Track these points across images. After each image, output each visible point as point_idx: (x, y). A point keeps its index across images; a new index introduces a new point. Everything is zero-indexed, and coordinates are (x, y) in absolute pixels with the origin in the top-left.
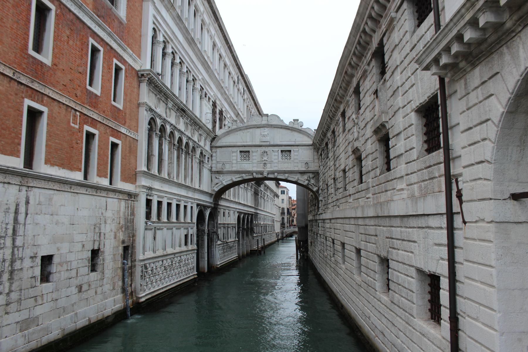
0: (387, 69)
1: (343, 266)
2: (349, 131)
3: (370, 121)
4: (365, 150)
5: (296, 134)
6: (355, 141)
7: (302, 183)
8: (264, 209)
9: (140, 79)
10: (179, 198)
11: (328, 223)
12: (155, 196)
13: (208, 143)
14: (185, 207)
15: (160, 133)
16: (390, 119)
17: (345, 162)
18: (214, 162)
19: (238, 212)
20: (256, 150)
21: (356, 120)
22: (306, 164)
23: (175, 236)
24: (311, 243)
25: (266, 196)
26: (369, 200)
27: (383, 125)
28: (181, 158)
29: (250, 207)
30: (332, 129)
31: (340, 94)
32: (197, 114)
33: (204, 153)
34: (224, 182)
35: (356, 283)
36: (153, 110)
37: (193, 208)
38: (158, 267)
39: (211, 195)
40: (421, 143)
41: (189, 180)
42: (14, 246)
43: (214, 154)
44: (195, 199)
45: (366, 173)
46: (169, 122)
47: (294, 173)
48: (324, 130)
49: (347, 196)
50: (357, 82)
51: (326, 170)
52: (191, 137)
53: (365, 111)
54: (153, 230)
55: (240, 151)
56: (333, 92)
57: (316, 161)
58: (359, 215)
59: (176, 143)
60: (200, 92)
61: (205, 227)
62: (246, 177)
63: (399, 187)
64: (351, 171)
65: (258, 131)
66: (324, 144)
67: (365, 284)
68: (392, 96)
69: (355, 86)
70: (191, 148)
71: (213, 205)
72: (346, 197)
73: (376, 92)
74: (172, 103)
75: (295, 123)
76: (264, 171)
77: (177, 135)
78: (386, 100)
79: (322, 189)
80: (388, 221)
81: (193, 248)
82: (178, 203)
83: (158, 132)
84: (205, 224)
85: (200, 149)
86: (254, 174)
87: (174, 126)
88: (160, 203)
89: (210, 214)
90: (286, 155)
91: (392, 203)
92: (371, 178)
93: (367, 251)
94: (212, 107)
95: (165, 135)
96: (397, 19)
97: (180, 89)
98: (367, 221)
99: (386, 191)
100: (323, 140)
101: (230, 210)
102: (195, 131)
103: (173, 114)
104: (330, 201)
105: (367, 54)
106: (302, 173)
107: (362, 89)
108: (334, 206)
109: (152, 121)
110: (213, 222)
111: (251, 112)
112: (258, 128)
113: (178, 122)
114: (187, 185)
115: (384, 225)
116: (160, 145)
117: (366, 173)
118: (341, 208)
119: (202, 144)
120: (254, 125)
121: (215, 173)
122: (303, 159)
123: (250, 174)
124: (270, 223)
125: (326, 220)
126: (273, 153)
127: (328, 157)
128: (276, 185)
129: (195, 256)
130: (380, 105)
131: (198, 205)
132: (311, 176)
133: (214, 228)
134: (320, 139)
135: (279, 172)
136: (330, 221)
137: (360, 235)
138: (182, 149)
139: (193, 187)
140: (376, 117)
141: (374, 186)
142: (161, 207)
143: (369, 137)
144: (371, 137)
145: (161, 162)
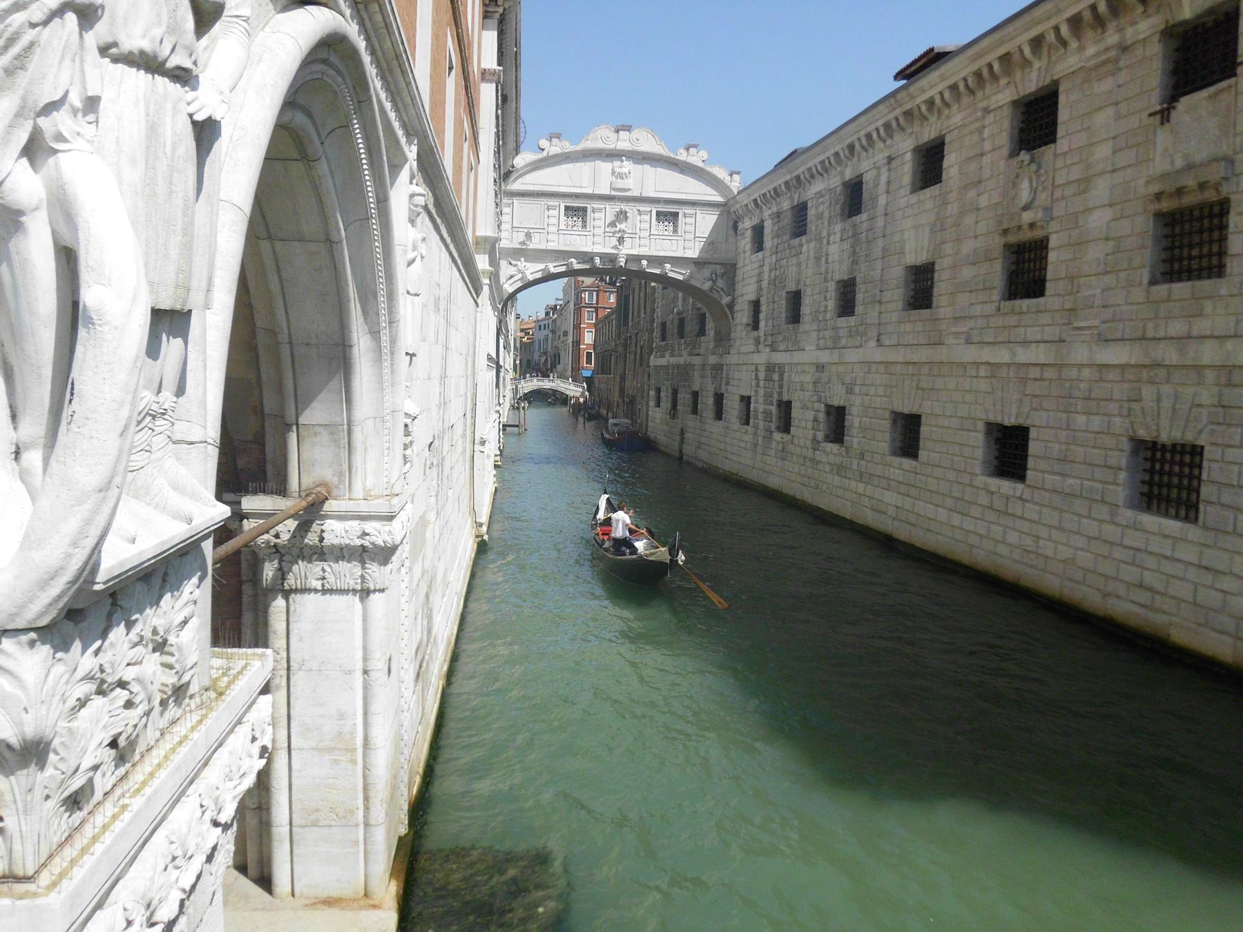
1: (907, 463)
6: (1026, 208)
7: (698, 285)
9: (485, 8)
31: (938, 101)
34: (528, 273)
35: (992, 493)
42: (445, 403)
43: (506, 210)
50: (1048, 81)
66: (786, 205)
76: (617, 254)
79: (756, 306)
86: (597, 260)
90: (666, 223)
105: (1134, 23)
126: (638, 217)
127: (803, 233)
135: (653, 260)
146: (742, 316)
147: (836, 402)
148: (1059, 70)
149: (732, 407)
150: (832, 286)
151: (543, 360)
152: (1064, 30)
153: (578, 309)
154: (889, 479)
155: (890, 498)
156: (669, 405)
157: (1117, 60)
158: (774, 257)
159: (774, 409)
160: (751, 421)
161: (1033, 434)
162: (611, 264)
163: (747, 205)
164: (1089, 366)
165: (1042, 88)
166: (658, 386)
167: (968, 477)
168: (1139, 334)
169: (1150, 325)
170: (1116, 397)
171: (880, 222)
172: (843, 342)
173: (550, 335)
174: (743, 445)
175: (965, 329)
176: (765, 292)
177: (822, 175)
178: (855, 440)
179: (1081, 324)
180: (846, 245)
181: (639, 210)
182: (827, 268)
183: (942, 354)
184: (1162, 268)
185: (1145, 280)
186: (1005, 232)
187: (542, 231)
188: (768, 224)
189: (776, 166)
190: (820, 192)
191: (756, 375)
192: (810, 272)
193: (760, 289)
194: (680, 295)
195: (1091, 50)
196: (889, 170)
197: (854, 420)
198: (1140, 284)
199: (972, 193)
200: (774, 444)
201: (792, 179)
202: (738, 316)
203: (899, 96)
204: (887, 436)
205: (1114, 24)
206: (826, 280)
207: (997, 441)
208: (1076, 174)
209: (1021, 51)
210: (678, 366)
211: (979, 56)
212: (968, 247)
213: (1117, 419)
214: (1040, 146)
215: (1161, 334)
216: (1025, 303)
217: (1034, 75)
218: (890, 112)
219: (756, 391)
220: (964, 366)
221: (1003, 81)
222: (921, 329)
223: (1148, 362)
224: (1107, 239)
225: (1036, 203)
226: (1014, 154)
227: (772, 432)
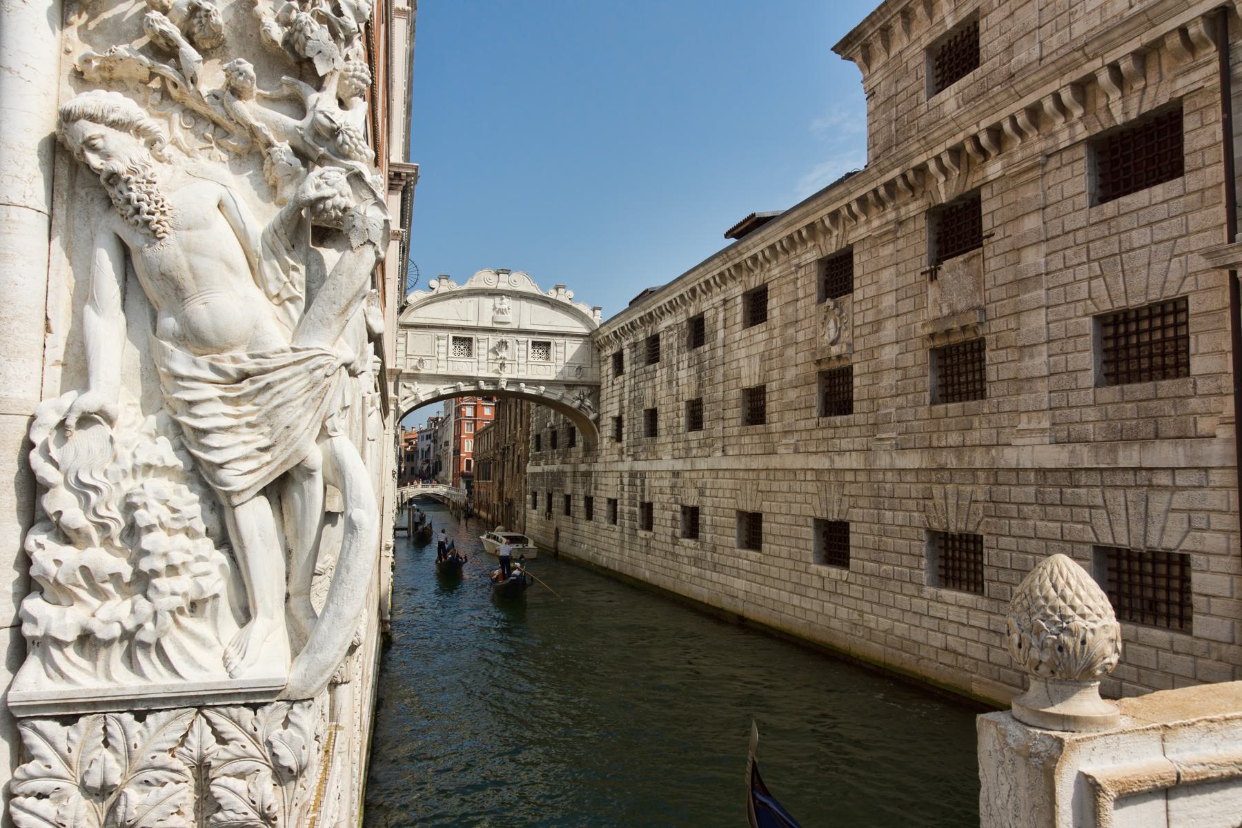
0: (985, 242)
1: (753, 554)
6: (833, 343)
11: (662, 478)
31: (760, 257)
40: (1100, 363)
50: (844, 245)
57: (596, 365)
62: (463, 387)
63: (1023, 425)
67: (868, 578)
79: (619, 421)
86: (482, 383)
90: (540, 351)
96: (1048, 168)
100: (634, 328)
105: (906, 204)
106: (570, 386)
120: (483, 289)
126: (517, 346)
127: (657, 360)
132: (586, 393)
135: (529, 383)
146: (607, 430)
147: (690, 503)
148: (853, 237)
149: (601, 508)
150: (683, 405)
151: (425, 467)
152: (855, 207)
153: (458, 424)
154: (738, 568)
155: (740, 584)
156: (545, 507)
157: (895, 232)
158: (633, 380)
159: (637, 510)
160: (618, 520)
161: (852, 527)
163: (608, 336)
164: (891, 470)
165: (841, 250)
166: (535, 490)
167: (804, 565)
168: (926, 444)
169: (935, 436)
170: (913, 496)
171: (720, 352)
172: (694, 452)
173: (432, 445)
174: (612, 541)
175: (793, 441)
176: (626, 410)
178: (708, 537)
179: (884, 436)
180: (693, 371)
182: (678, 391)
183: (775, 462)
184: (939, 392)
185: (928, 401)
186: (819, 362)
188: (626, 352)
189: (631, 303)
190: (669, 327)
191: (621, 481)
192: (664, 393)
193: (621, 408)
194: (552, 411)
195: (876, 223)
196: (725, 310)
197: (706, 518)
198: (924, 404)
199: (791, 331)
200: (639, 541)
203: (731, 252)
204: (735, 532)
205: (892, 204)
206: (677, 400)
207: (825, 533)
208: (870, 317)
209: (823, 222)
210: (552, 473)
211: (790, 224)
212: (791, 374)
213: (916, 514)
214: (841, 295)
215: (943, 444)
216: (838, 419)
217: (834, 240)
219: (622, 495)
220: (794, 471)
221: (810, 244)
222: (758, 441)
223: (935, 466)
224: (897, 369)
225: (842, 339)
226: (821, 301)
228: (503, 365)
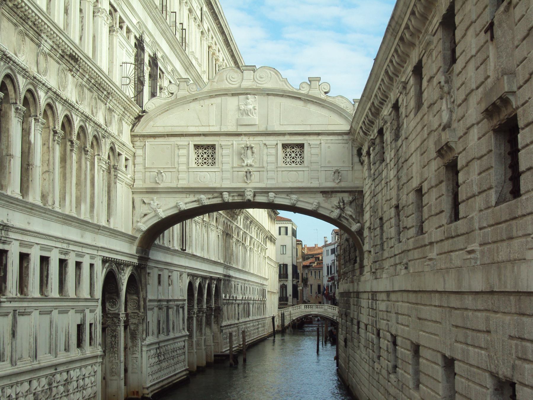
2: (430, 106)
3: (477, 88)
4: (464, 149)
5: (313, 108)
6: (444, 129)
8: (244, 266)
10: (65, 246)
12: (14, 242)
13: (127, 128)
14: (78, 265)
15: (25, 109)
16: (520, 88)
17: (422, 174)
18: (139, 168)
19: (189, 275)
20: (230, 143)
21: (446, 85)
22: (336, 174)
23: (57, 327)
24: (345, 341)
25: (248, 239)
26: (472, 256)
27: (504, 101)
28: (68, 162)
29: (215, 263)
30: (393, 101)
31: (411, 27)
32: (103, 63)
33: (117, 150)
36: (11, 59)
37: (95, 266)
38: (20, 394)
39: (131, 238)
41: (85, 208)
43: (139, 152)
44: (98, 248)
45: (468, 199)
46: (44, 84)
47: (312, 192)
48: (376, 103)
49: (425, 246)
50: (448, 4)
51: (379, 188)
52: (91, 116)
53: (465, 67)
54: (10, 316)
55: (195, 145)
56: (397, 23)
57: (358, 166)
58: (451, 286)
59: (58, 128)
60: (110, 17)
61: (119, 309)
62: (206, 200)
64: (434, 194)
65: (232, 102)
66: (376, 131)
68: (524, 38)
69: (444, 12)
70: (90, 138)
71: (136, 261)
72: (422, 247)
73: (490, 28)
74: (51, 43)
75: (312, 86)
76: (245, 188)
77: (61, 111)
78: (511, 46)
80: (513, 302)
81: (95, 354)
82: (63, 257)
83: (20, 106)
84: (120, 302)
85: (108, 141)
86: (226, 195)
87: (55, 93)
88: (24, 257)
89: (132, 280)
90: (293, 155)
91: (524, 267)
92: (477, 209)
93: (467, 364)
94: (135, 50)
95: (36, 111)
97: (66, 11)
98: (469, 301)
99: (511, 238)
101: (171, 271)
102: (98, 101)
103: (53, 66)
104: (386, 254)
107: (460, 18)
108: (396, 265)
109: (8, 83)
110: (135, 297)
111: (216, 60)
112: (233, 95)
113: (63, 85)
114: (82, 217)
115: (506, 311)
116: (26, 132)
117: (468, 199)
118: (411, 271)
119: (113, 129)
121: (141, 193)
122: (329, 162)
123: (216, 195)
124: (256, 297)
125: (378, 295)
126: (265, 151)
128: (270, 216)
129: (98, 368)
130: (499, 57)
131: (105, 261)
133: (139, 308)
134: (367, 121)
135: (279, 191)
136: (388, 296)
137: (454, 329)
138: (72, 142)
139: (95, 222)
140: (489, 80)
141: (484, 228)
142: (27, 267)
143: (474, 122)
144: (478, 123)
145: (27, 169)
149: (362, 331)
150: (393, 211)
162: (240, 198)
163: (359, 133)
177: (386, 101)
181: (265, 144)
185: (493, 203)
186: (440, 153)
187: (174, 170)
201: (372, 107)
202: (365, 242)
218: (395, 39)
227: (375, 362)
228: (248, 173)
